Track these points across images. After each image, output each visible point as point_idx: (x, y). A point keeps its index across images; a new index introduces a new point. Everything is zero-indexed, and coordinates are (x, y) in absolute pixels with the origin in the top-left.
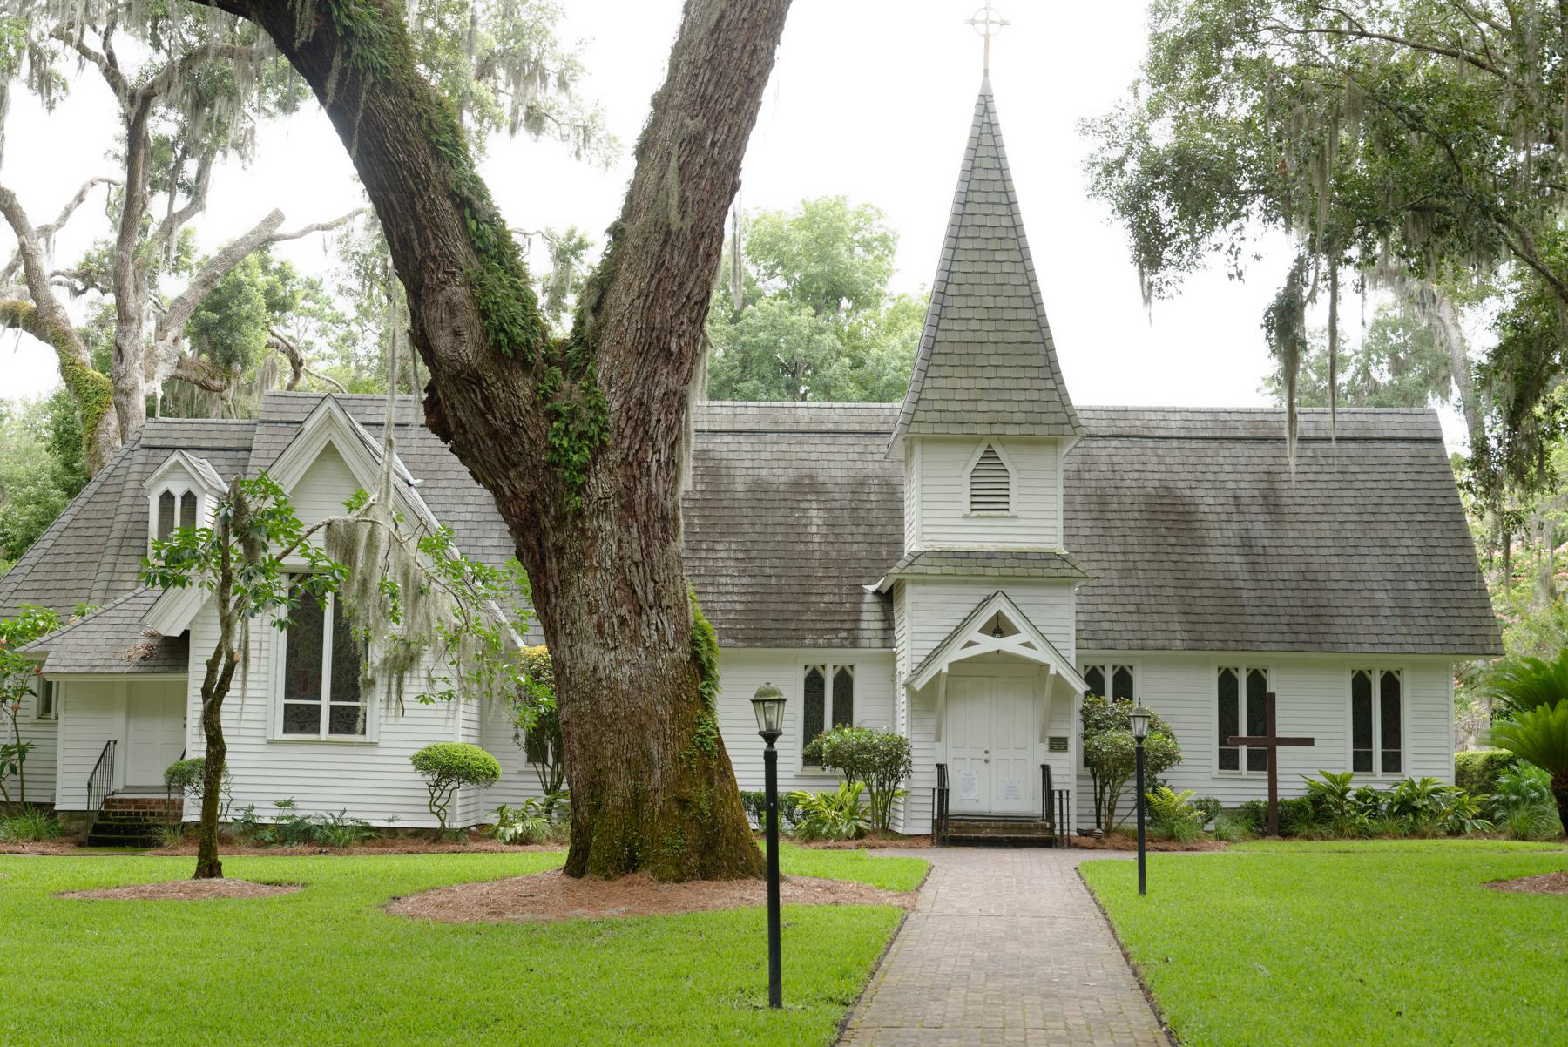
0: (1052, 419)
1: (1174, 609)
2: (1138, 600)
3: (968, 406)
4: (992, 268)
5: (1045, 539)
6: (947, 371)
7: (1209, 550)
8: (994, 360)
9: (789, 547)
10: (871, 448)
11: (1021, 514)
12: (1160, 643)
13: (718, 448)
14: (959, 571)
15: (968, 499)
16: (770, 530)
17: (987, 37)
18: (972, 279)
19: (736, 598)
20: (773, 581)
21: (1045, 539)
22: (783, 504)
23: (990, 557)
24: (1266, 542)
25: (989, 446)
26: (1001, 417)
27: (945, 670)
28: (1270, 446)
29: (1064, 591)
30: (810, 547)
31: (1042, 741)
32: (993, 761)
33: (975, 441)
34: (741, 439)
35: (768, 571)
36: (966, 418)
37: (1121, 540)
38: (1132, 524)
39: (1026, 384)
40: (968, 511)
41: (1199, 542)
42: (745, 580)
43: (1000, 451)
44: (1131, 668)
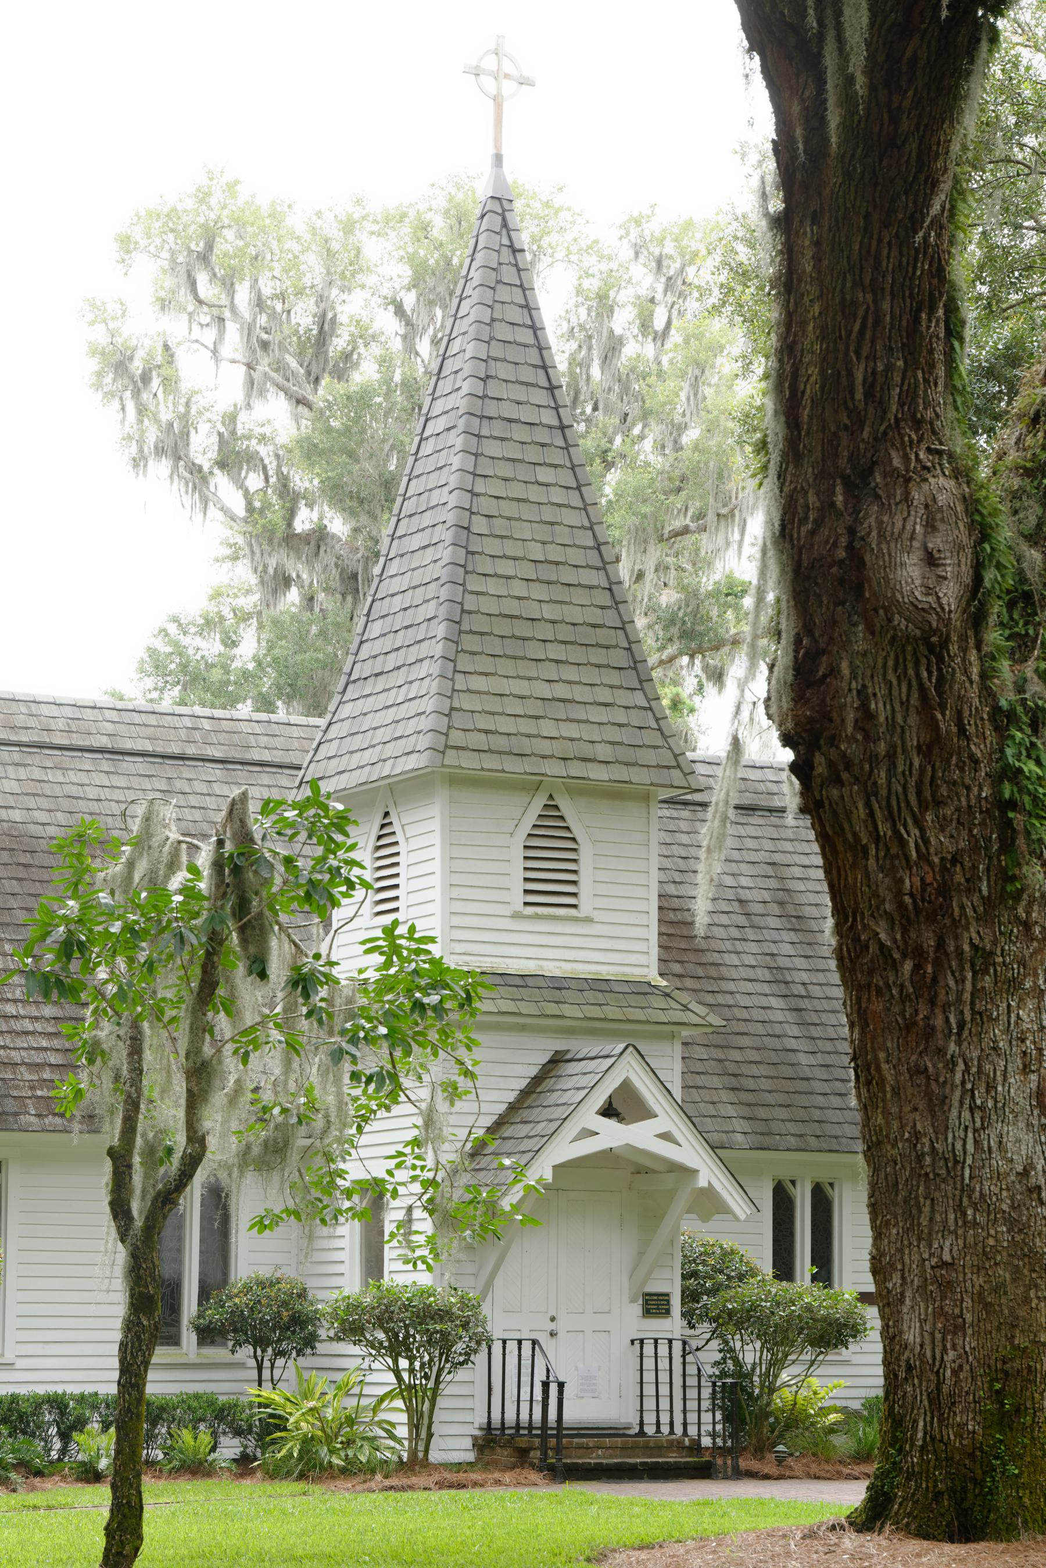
0: (650, 757)
1: (716, 1081)
3: (526, 726)
4: (534, 494)
5: (632, 959)
6: (483, 664)
7: (731, 986)
8: (555, 652)
10: (179, 785)
11: (597, 916)
14: (525, 1008)
17: (498, 101)
18: (509, 509)
19: (44, 1043)
21: (632, 959)
23: (558, 985)
24: (804, 977)
25: (551, 797)
26: (571, 749)
27: (548, 1176)
28: (761, 821)
31: (633, 1301)
33: (532, 786)
36: (526, 745)
39: (604, 695)
40: (520, 907)
41: (713, 972)
43: (567, 807)
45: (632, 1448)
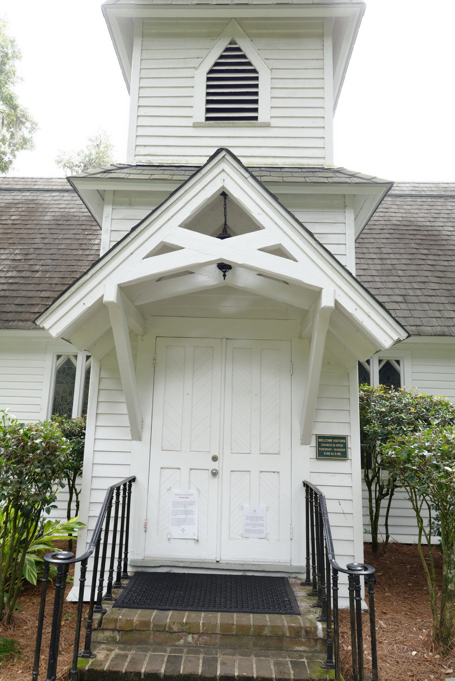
2: (403, 292)
9: (68, 252)
11: (274, 122)
12: (439, 329)
13: (44, 198)
15: (203, 106)
16: (57, 242)
20: (38, 275)
22: (79, 227)
29: (339, 217)
30: (87, 252)
31: (305, 441)
32: (224, 473)
34: (66, 194)
35: (37, 268)
37: (377, 251)
38: (384, 241)
42: (9, 274)
44: (398, 362)
45: (237, 635)
